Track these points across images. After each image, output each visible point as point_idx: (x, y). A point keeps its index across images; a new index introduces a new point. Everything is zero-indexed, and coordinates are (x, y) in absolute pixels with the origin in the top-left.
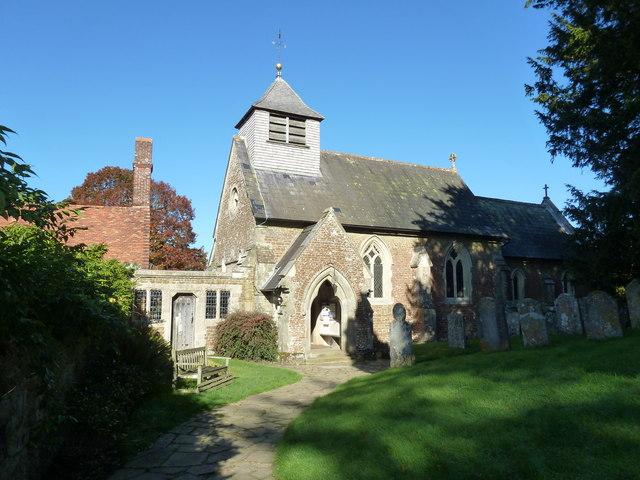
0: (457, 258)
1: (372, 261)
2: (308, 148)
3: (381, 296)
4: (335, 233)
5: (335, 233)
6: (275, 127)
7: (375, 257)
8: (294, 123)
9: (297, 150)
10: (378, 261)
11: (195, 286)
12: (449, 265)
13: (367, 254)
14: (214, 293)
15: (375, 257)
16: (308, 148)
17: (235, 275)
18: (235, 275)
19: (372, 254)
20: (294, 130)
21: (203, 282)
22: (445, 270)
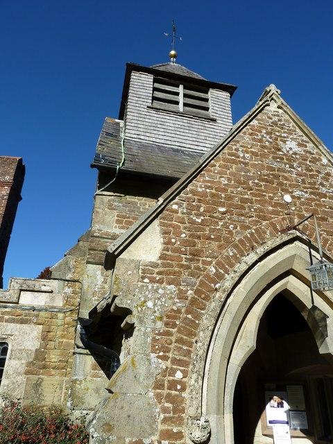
9: (197, 124)
17: (27, 299)
18: (27, 299)
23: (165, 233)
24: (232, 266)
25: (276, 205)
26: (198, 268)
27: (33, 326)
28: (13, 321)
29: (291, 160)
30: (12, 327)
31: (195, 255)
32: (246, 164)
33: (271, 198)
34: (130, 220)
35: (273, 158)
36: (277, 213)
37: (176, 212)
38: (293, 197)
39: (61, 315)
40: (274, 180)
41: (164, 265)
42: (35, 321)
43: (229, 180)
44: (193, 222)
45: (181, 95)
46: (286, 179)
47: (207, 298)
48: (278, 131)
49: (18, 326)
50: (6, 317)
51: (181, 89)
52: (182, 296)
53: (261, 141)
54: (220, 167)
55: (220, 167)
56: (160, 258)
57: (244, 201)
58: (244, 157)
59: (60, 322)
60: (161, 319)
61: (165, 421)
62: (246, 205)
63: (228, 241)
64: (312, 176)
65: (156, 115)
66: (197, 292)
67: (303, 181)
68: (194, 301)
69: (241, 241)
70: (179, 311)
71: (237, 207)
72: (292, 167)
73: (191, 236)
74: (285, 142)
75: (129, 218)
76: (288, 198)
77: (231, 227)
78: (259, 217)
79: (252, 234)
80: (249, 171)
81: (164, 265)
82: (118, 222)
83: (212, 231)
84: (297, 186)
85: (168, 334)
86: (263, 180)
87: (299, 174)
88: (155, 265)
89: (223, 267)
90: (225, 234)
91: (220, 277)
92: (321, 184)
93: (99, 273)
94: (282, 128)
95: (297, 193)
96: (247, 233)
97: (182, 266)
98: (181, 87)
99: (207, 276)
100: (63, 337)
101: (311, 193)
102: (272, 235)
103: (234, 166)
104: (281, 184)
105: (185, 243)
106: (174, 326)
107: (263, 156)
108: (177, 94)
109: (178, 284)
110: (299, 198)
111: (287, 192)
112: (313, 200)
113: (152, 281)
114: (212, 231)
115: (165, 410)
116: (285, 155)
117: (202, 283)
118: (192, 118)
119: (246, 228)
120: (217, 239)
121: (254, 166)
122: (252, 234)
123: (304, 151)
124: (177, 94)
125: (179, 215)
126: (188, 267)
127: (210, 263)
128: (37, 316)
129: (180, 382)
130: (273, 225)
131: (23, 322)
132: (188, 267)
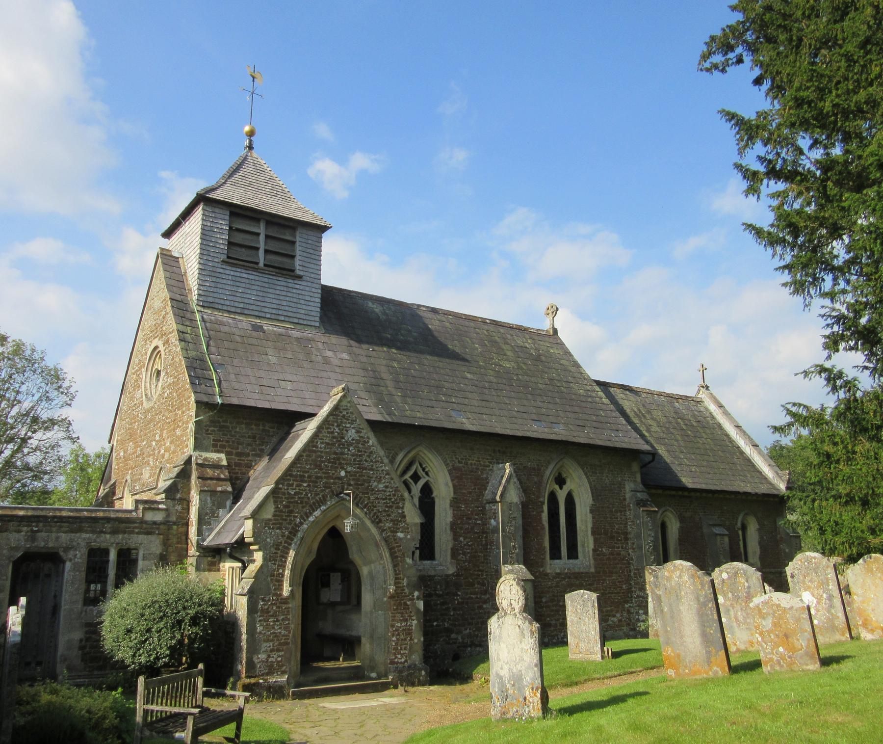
0: (566, 488)
1: (416, 489)
2: (300, 277)
3: (576, 557)
4: (352, 434)
5: (352, 434)
6: (239, 238)
7: (421, 483)
8: (273, 232)
9: (282, 282)
10: (427, 490)
11: (64, 537)
12: (553, 498)
13: (407, 476)
14: (106, 552)
15: (421, 483)
16: (300, 277)
19: (416, 478)
20: (274, 246)
21: (80, 530)
22: (545, 508)
23: (275, 502)
24: (308, 517)
25: (336, 478)
26: (291, 520)
27: (156, 536)
28: (138, 533)
29: (350, 444)
30: (141, 537)
31: (291, 512)
32: (321, 452)
33: (333, 474)
34: (224, 443)
35: (339, 445)
36: (334, 483)
37: (281, 489)
38: (346, 472)
39: (175, 527)
40: (338, 462)
41: (275, 520)
42: (157, 532)
43: (311, 465)
44: (289, 494)
45: (262, 238)
46: (344, 459)
47: (295, 535)
48: (346, 423)
49: (145, 536)
50: (137, 531)
51: (261, 229)
52: (283, 536)
53: (332, 433)
54: (306, 456)
55: (306, 456)
56: (274, 516)
57: (317, 478)
58: (321, 448)
59: (175, 533)
60: (273, 546)
61: (275, 589)
62: (318, 481)
63: (307, 503)
64: (360, 456)
65: (232, 273)
66: (290, 533)
67: (355, 460)
68: (288, 537)
69: (314, 503)
70: (281, 543)
71: (313, 482)
72: (349, 450)
73: (288, 502)
74: (347, 431)
75: (222, 441)
76: (343, 473)
77: (309, 495)
78: (324, 487)
79: (320, 498)
80: (323, 457)
81: (275, 520)
82: (215, 446)
83: (299, 498)
84: (350, 465)
85: (276, 553)
86: (330, 462)
87: (353, 455)
88: (270, 520)
89: (304, 519)
90: (306, 500)
91: (301, 524)
92: (366, 461)
93: (209, 498)
94: (348, 420)
95: (349, 468)
96: (317, 498)
97: (283, 520)
98: (262, 225)
99: (295, 524)
100: (178, 543)
101: (358, 468)
102: (331, 498)
103: (314, 454)
104: (340, 464)
105: (285, 506)
106: (279, 549)
107: (333, 444)
108: (258, 234)
109: (280, 528)
110: (349, 472)
111: (343, 468)
112: (358, 472)
113: (269, 528)
114: (299, 498)
115: (274, 585)
116: (346, 442)
117: (293, 528)
118: (273, 275)
119: (317, 494)
120: (302, 503)
121: (326, 453)
122: (320, 498)
123: (359, 436)
124: (258, 234)
125: (283, 490)
126: (286, 520)
127: (297, 517)
128: (158, 529)
129: (281, 574)
130: (332, 492)
131: (148, 533)
132: (286, 520)
